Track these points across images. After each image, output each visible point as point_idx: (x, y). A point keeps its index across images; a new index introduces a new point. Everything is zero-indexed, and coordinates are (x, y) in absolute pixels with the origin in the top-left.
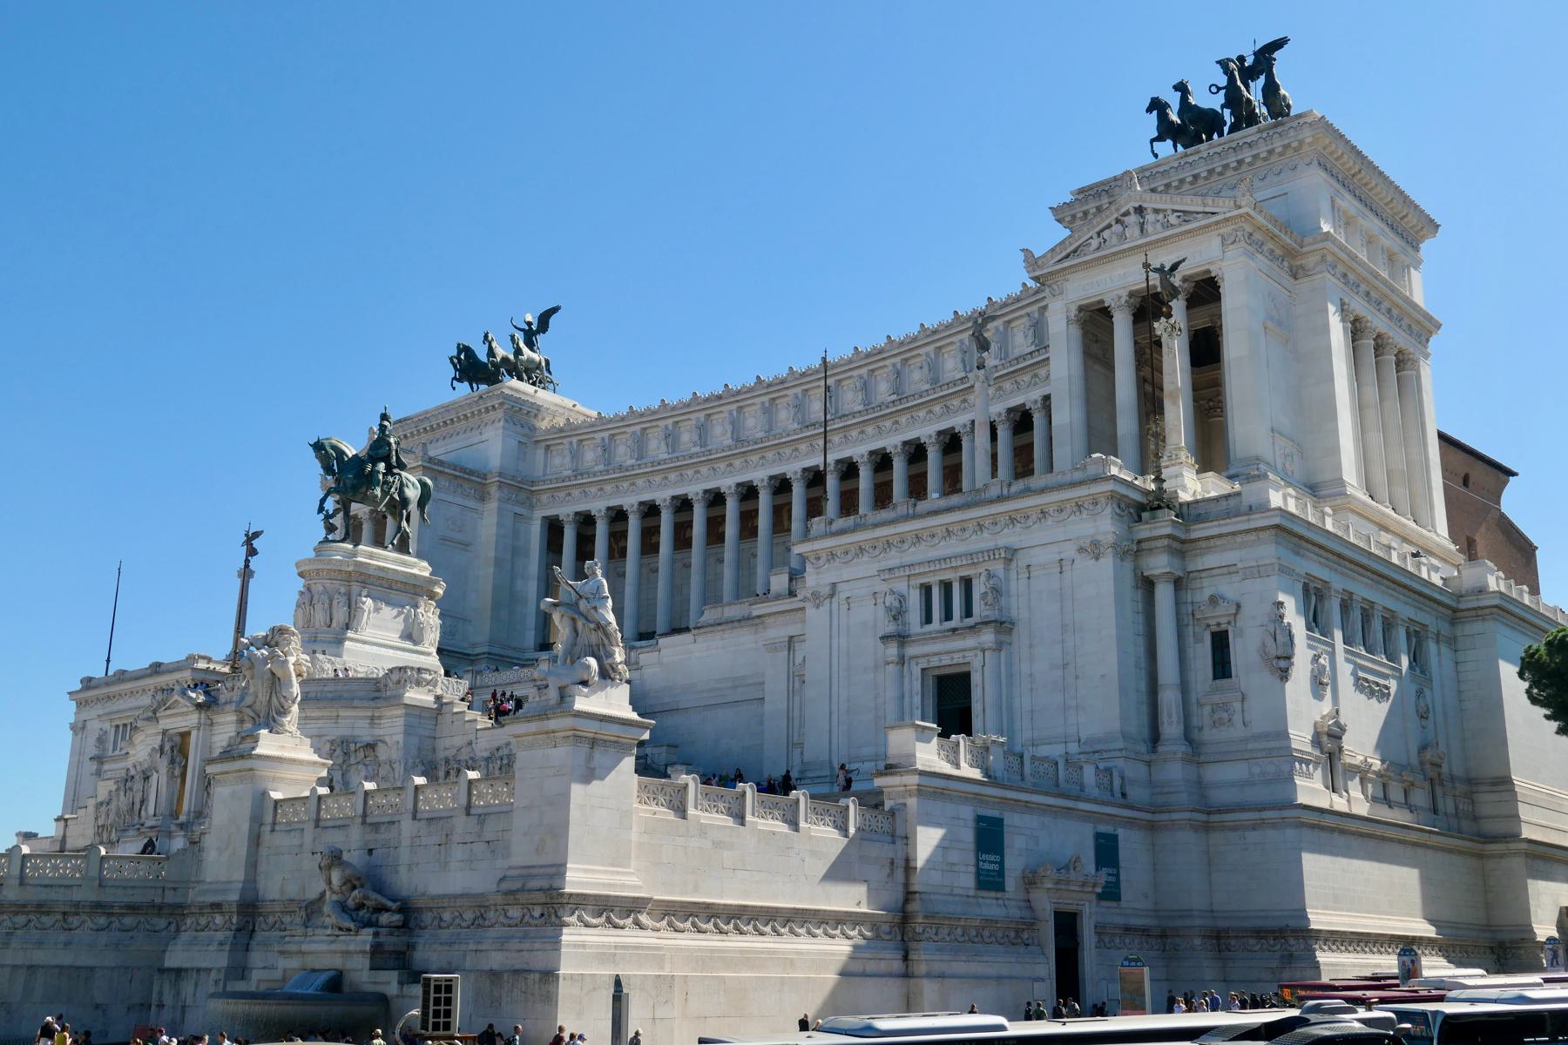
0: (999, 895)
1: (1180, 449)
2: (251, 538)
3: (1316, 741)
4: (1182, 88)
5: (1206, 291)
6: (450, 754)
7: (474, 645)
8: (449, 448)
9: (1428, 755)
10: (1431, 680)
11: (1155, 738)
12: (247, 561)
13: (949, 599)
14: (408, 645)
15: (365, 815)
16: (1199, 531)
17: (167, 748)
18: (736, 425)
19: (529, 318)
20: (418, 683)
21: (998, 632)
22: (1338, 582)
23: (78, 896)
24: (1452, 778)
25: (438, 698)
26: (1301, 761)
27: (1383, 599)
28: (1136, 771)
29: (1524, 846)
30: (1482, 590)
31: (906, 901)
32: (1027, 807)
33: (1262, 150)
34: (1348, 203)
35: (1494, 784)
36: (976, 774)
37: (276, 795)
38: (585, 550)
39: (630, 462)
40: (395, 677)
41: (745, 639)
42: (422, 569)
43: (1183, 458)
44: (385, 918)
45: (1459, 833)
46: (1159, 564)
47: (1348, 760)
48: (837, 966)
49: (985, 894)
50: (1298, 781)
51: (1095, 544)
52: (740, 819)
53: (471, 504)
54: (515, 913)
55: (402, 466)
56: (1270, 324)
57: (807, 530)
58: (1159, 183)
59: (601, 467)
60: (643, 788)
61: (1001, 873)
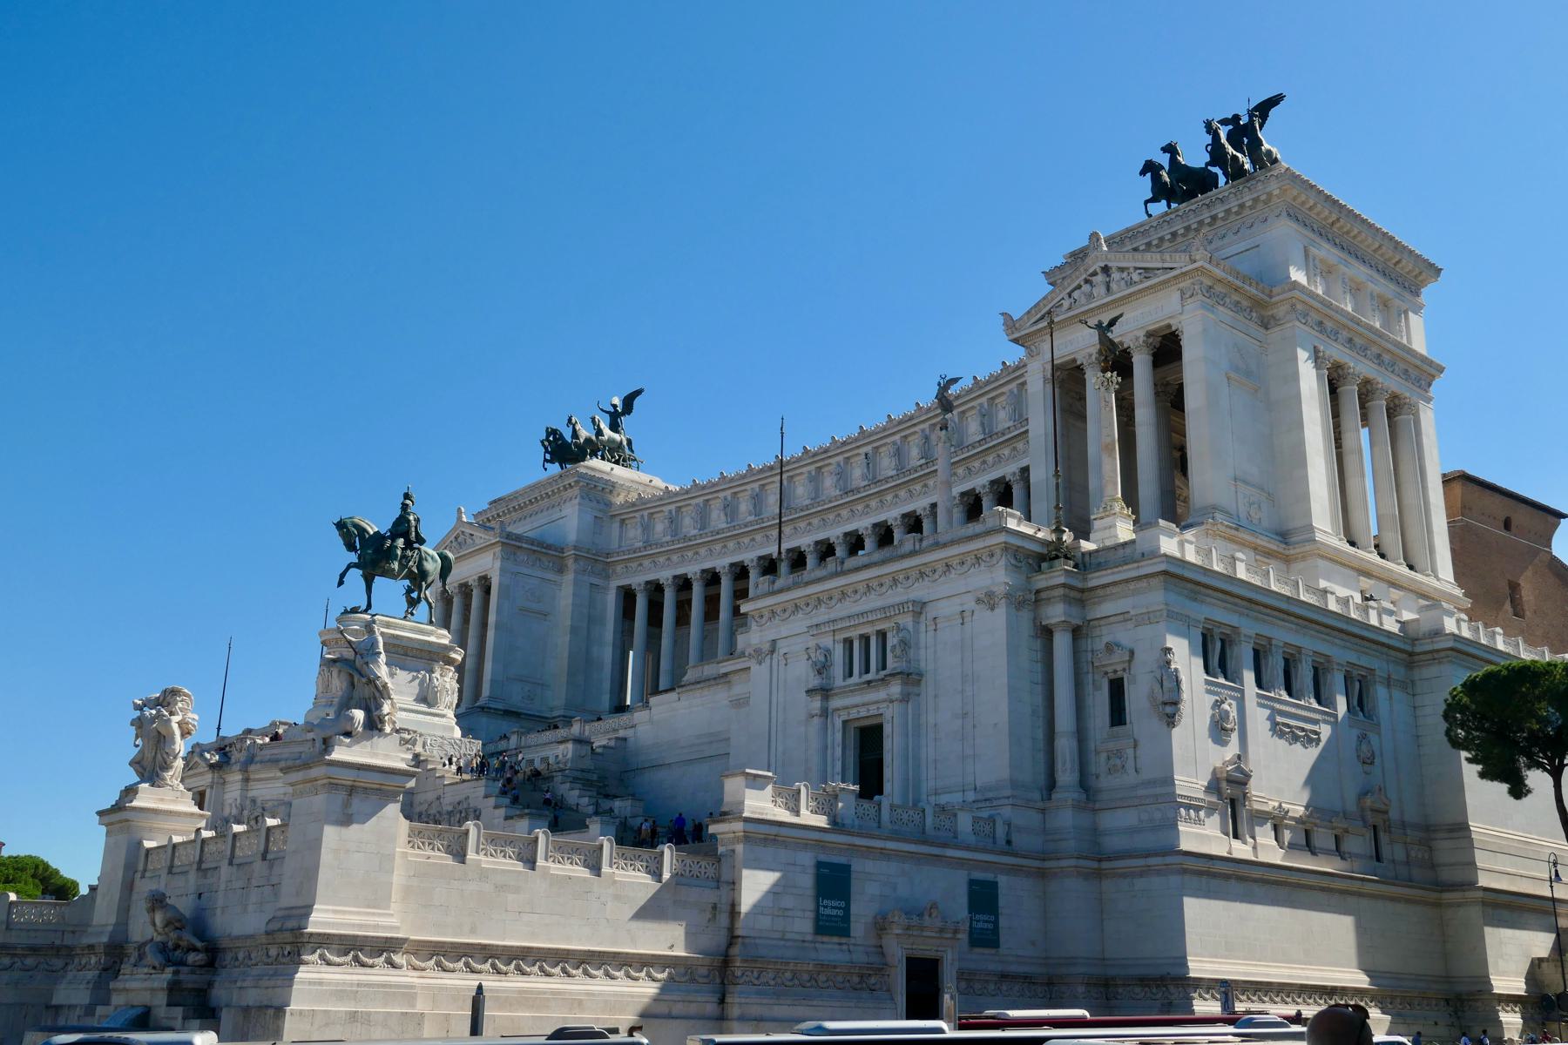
0: (844, 940)
1: (1115, 500)
3: (1214, 787)
4: (1170, 149)
7: (552, 709)
8: (536, 525)
9: (1368, 801)
10: (1379, 725)
11: (1051, 785)
13: (871, 653)
14: (423, 708)
15: (201, 861)
16: (1096, 579)
19: (616, 401)
21: (905, 683)
22: (1250, 628)
24: (1404, 825)
26: (1188, 807)
27: (1310, 644)
28: (1031, 818)
29: (1480, 894)
30: (1438, 633)
31: (730, 945)
33: (1233, 204)
34: (1325, 251)
36: (821, 821)
37: (148, 844)
39: (695, 532)
42: (442, 637)
43: (1117, 509)
44: (192, 958)
45: (1409, 882)
46: (1056, 613)
47: (1256, 806)
48: (639, 1008)
49: (826, 939)
50: (1182, 827)
51: (990, 595)
52: (531, 863)
53: (550, 576)
54: (273, 952)
55: (421, 541)
56: (1232, 375)
58: (1140, 243)
59: (668, 538)
60: (413, 834)
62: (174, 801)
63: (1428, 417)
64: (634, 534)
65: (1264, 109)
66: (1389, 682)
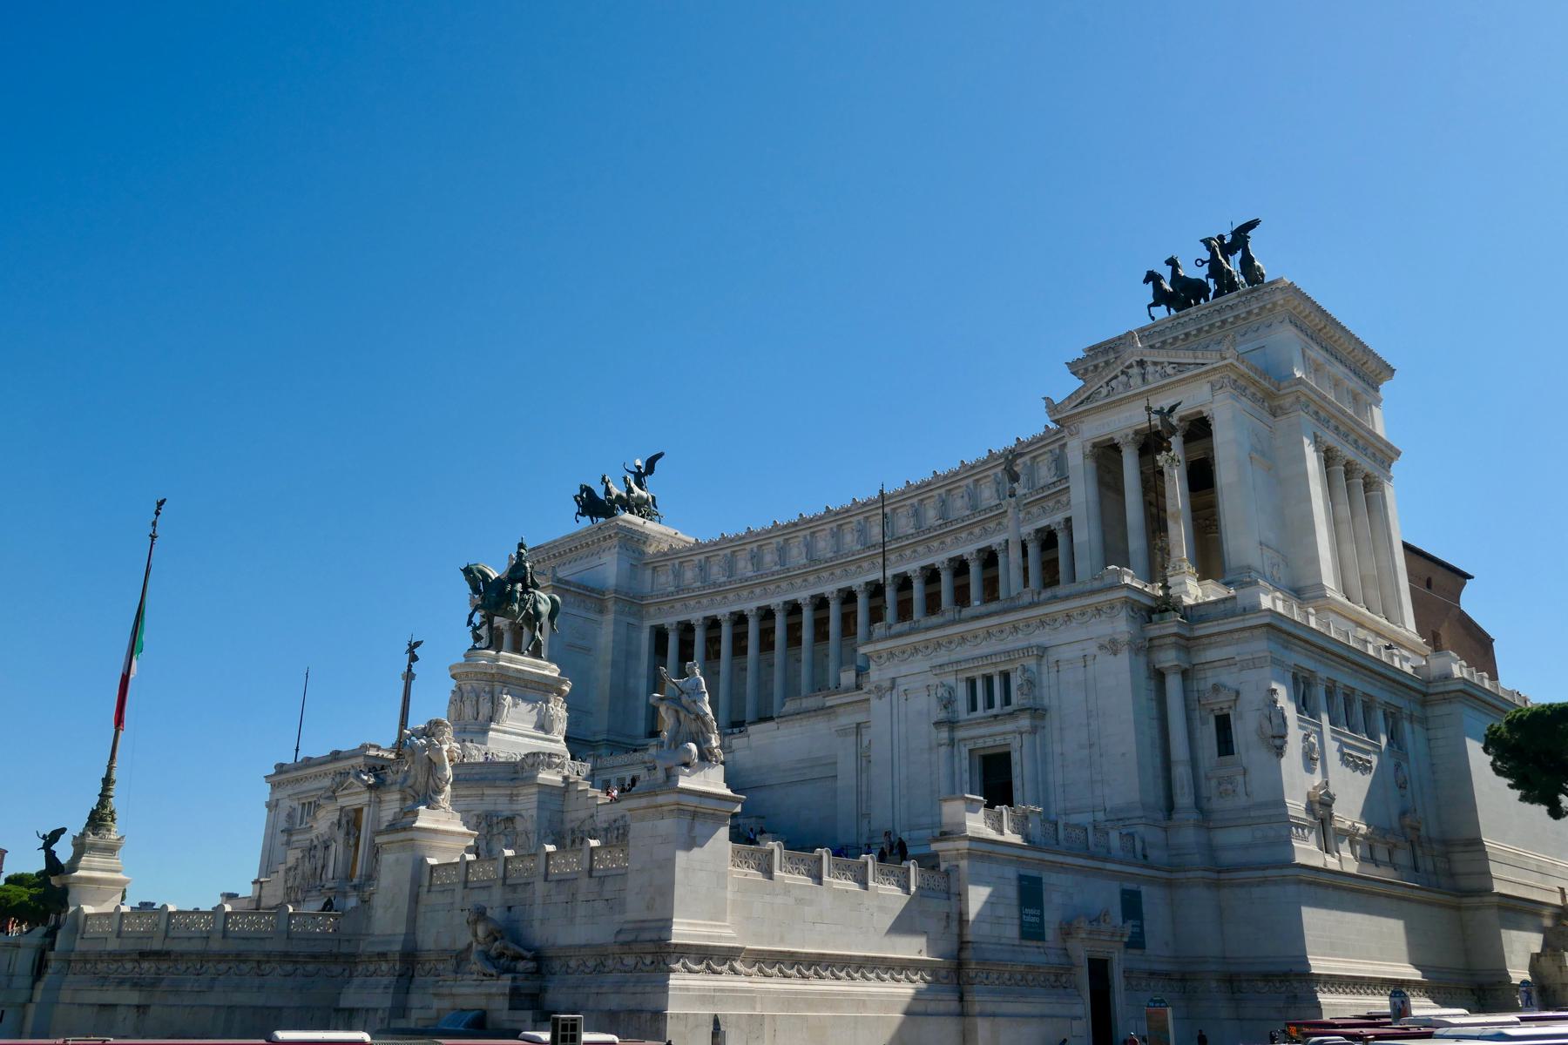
2: (413, 646)
3: (1310, 809)
4: (1172, 262)
5: (1199, 429)
6: (575, 825)
7: (595, 734)
9: (1408, 821)
11: (1170, 807)
12: (410, 667)
13: (991, 690)
14: (541, 734)
15: (505, 878)
16: (1203, 630)
17: (344, 822)
18: (809, 547)
19: (639, 463)
20: (549, 766)
21: (1033, 718)
23: (269, 946)
24: (1430, 840)
25: (566, 778)
26: (1297, 826)
27: (1361, 685)
28: (1154, 835)
29: (1496, 899)
30: (1448, 677)
31: (961, 949)
33: (1242, 311)
34: (1316, 353)
35: (1466, 845)
36: (1017, 839)
37: (432, 861)
38: (686, 654)
39: (723, 579)
40: (530, 761)
41: (820, 726)
42: (552, 671)
44: (521, 965)
46: (1168, 658)
47: (1338, 825)
48: (902, 1007)
49: (1029, 943)
51: (1113, 642)
52: (818, 879)
54: (630, 961)
55: (536, 586)
57: (870, 633)
58: (1157, 341)
60: (736, 853)
61: (1041, 924)
62: (446, 822)
63: (1391, 492)
66: (1411, 718)
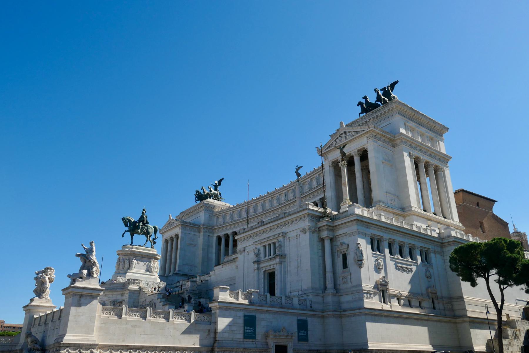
0: (254, 340)
1: (347, 200)
3: (376, 287)
4: (365, 98)
6: (141, 304)
9: (430, 290)
10: (432, 266)
11: (325, 288)
16: (337, 223)
18: (263, 206)
20: (134, 283)
21: (280, 258)
22: (386, 236)
24: (442, 297)
25: (140, 287)
27: (408, 241)
28: (320, 299)
29: (468, 319)
30: (450, 236)
31: (214, 343)
32: (262, 311)
33: (383, 111)
34: (411, 124)
35: (458, 299)
36: (246, 302)
37: (35, 317)
39: (237, 219)
45: (445, 316)
46: (325, 234)
47: (391, 293)
49: (247, 340)
50: (365, 300)
53: (196, 234)
55: (148, 223)
56: (384, 161)
61: (255, 333)
63: (447, 172)
64: (221, 220)
65: (393, 85)
66: (435, 252)
